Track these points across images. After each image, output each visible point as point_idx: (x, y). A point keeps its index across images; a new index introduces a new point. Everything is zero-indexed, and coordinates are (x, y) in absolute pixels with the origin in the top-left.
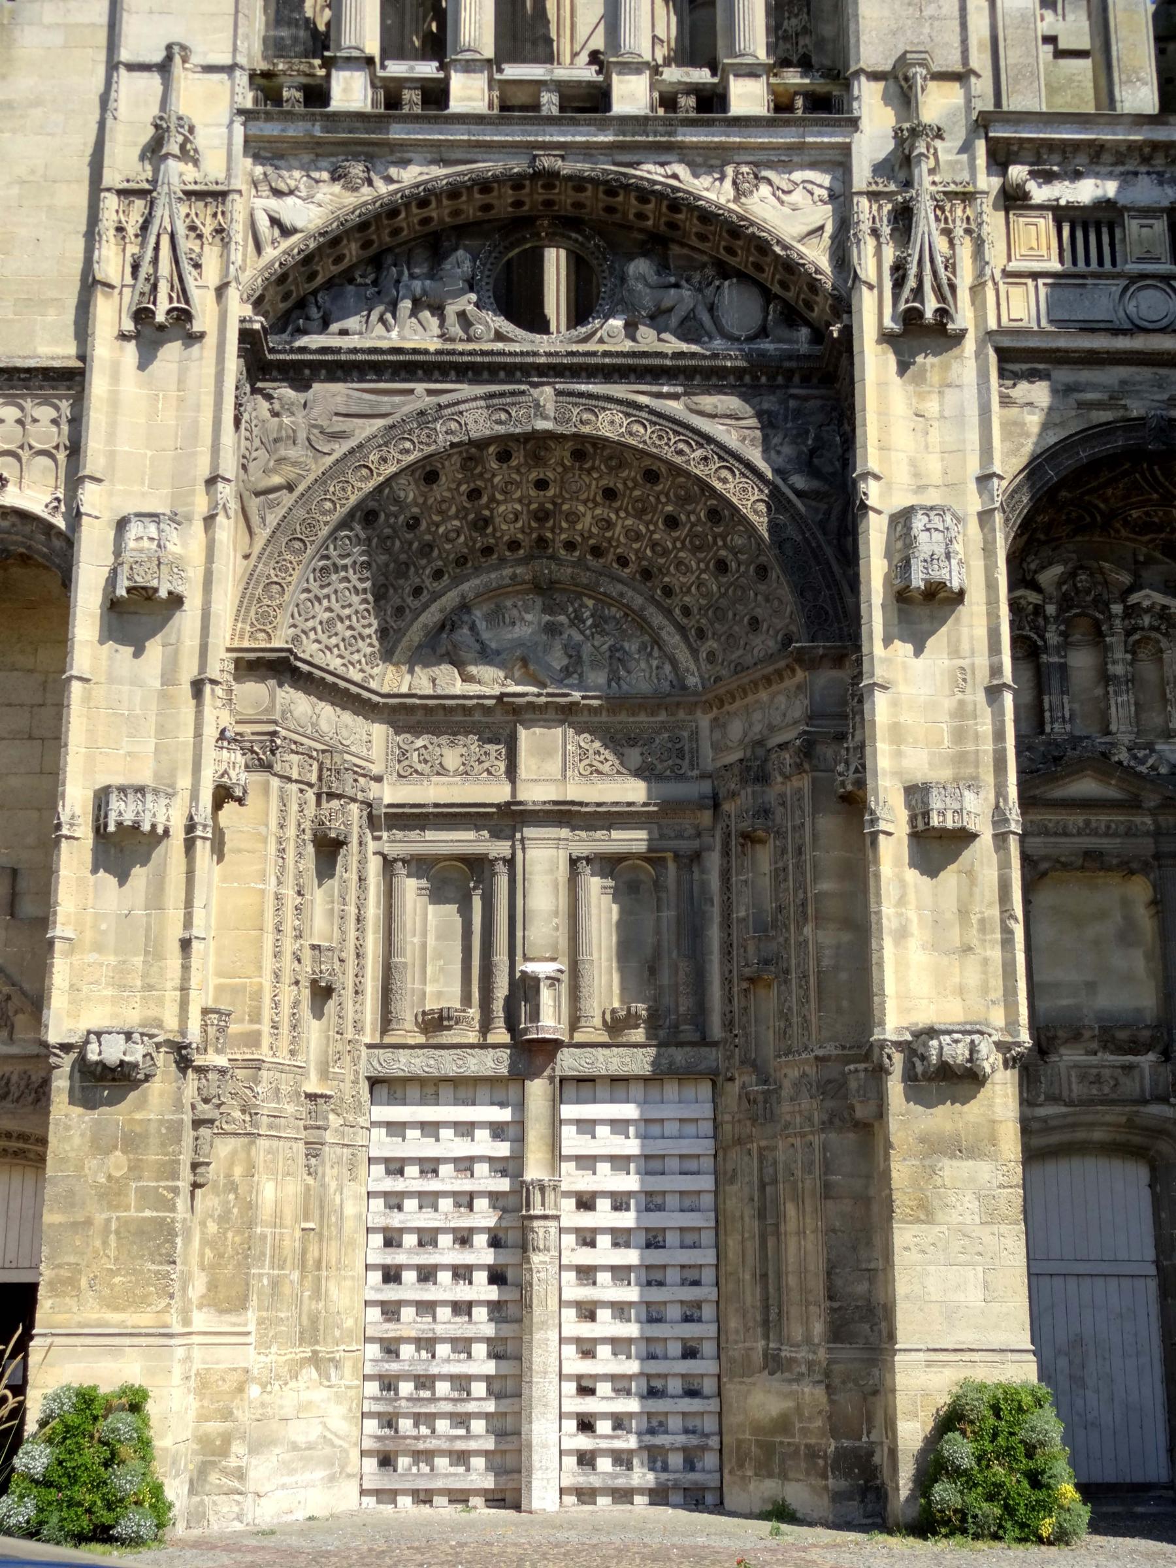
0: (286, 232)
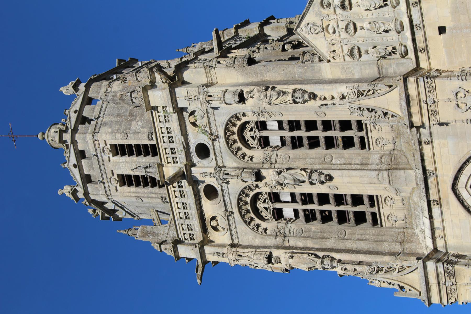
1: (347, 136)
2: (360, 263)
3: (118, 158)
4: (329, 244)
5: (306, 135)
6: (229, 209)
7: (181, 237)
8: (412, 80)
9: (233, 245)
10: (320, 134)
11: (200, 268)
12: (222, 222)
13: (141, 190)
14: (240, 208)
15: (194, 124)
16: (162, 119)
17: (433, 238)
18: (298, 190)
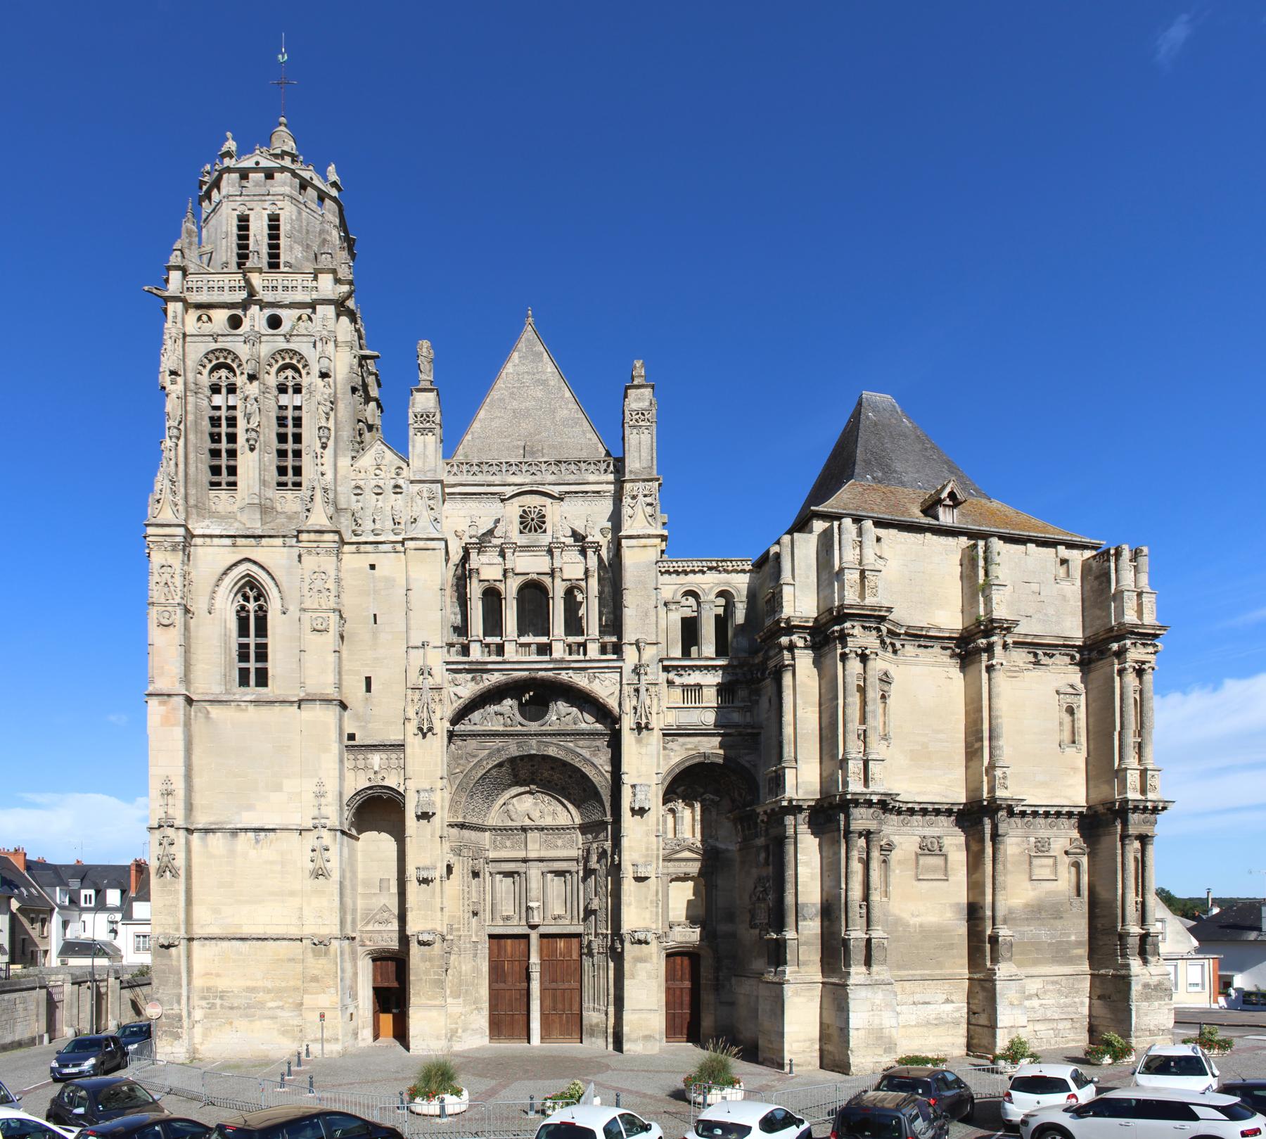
0: (460, 698)
1: (288, 472)
2: (177, 465)
3: (266, 222)
4: (191, 437)
5: (289, 431)
6: (220, 339)
7: (190, 278)
8: (336, 538)
9: (185, 335)
10: (290, 446)
11: (158, 292)
12: (207, 328)
13: (234, 240)
14: (221, 350)
15: (300, 318)
16: (305, 283)
17: (204, 536)
18: (239, 414)
